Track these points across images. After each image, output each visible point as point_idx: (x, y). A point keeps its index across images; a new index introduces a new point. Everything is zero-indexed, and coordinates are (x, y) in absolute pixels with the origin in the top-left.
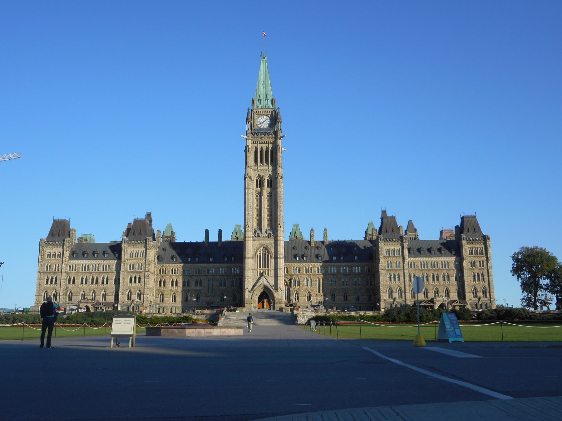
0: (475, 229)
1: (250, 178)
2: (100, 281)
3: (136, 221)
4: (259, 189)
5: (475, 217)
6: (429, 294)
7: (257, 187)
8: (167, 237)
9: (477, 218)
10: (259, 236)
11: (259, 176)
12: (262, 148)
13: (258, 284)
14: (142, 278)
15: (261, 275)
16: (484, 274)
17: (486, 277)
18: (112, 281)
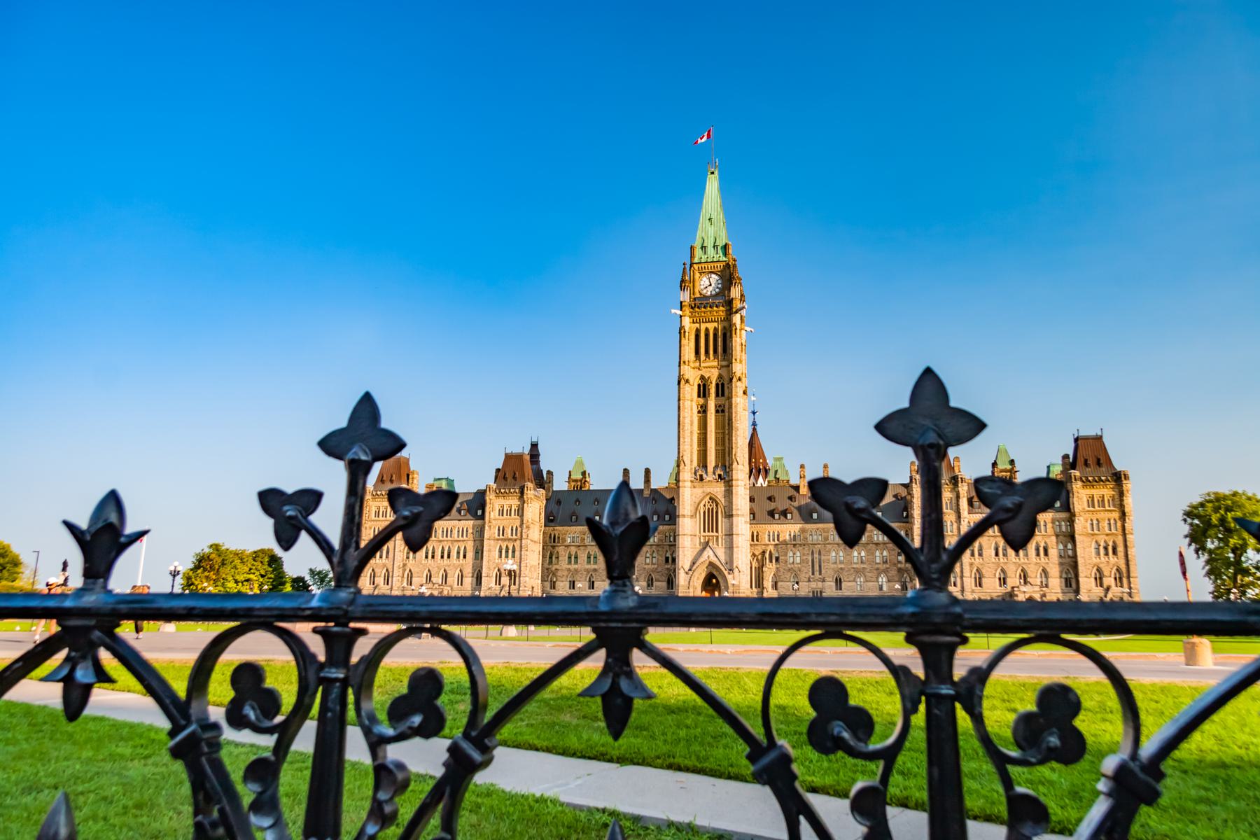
0: (1099, 460)
1: (687, 381)
2: (454, 554)
3: (509, 458)
4: (701, 401)
5: (1101, 437)
6: (1008, 580)
7: (699, 396)
8: (576, 481)
9: (1104, 439)
10: (702, 479)
11: (702, 378)
12: (707, 329)
13: (701, 560)
14: (517, 549)
15: (706, 545)
16: (1119, 546)
17: (1120, 549)
18: (470, 555)
